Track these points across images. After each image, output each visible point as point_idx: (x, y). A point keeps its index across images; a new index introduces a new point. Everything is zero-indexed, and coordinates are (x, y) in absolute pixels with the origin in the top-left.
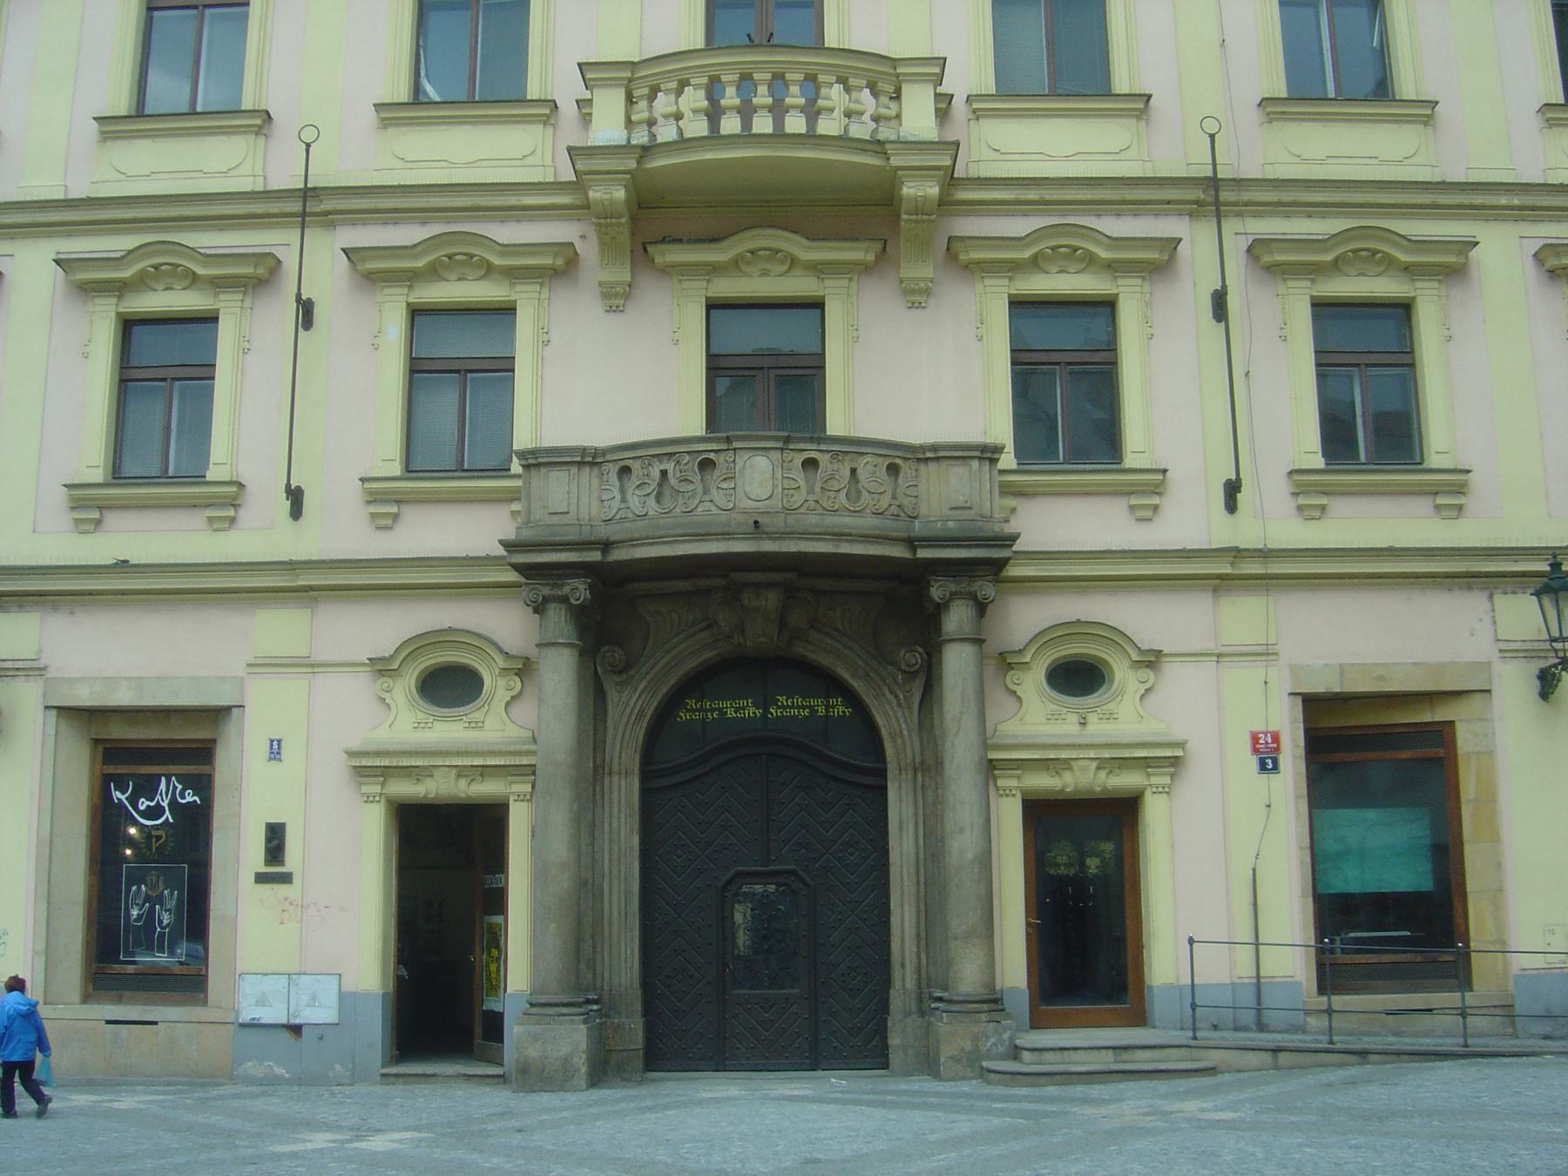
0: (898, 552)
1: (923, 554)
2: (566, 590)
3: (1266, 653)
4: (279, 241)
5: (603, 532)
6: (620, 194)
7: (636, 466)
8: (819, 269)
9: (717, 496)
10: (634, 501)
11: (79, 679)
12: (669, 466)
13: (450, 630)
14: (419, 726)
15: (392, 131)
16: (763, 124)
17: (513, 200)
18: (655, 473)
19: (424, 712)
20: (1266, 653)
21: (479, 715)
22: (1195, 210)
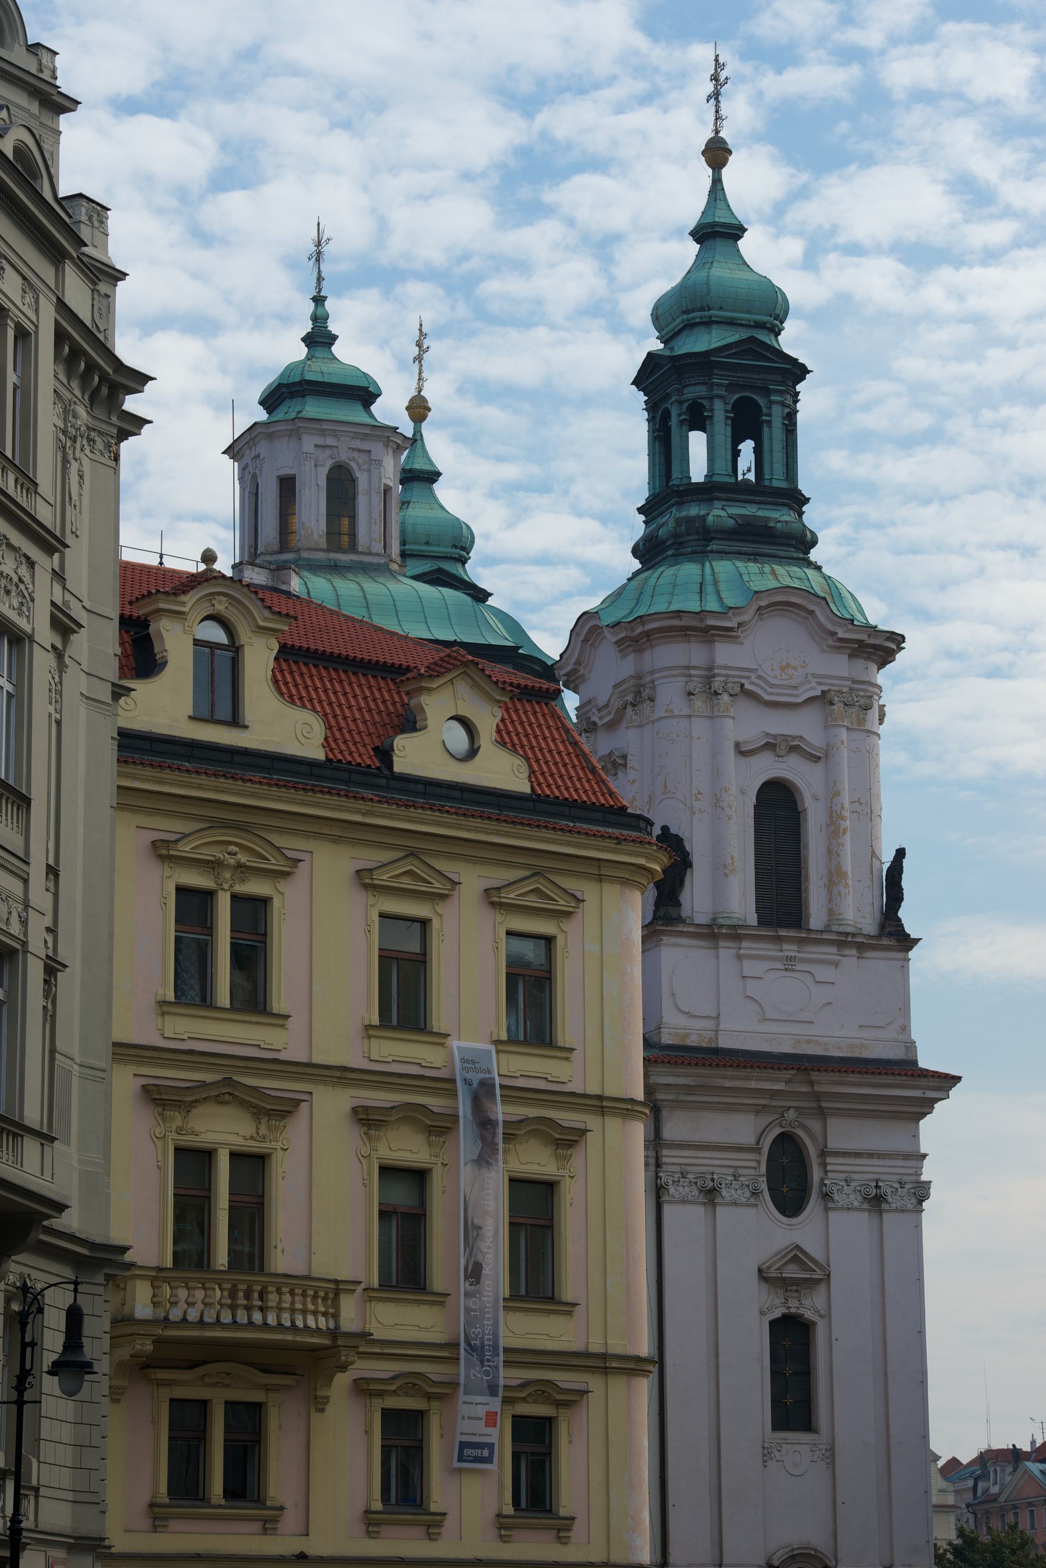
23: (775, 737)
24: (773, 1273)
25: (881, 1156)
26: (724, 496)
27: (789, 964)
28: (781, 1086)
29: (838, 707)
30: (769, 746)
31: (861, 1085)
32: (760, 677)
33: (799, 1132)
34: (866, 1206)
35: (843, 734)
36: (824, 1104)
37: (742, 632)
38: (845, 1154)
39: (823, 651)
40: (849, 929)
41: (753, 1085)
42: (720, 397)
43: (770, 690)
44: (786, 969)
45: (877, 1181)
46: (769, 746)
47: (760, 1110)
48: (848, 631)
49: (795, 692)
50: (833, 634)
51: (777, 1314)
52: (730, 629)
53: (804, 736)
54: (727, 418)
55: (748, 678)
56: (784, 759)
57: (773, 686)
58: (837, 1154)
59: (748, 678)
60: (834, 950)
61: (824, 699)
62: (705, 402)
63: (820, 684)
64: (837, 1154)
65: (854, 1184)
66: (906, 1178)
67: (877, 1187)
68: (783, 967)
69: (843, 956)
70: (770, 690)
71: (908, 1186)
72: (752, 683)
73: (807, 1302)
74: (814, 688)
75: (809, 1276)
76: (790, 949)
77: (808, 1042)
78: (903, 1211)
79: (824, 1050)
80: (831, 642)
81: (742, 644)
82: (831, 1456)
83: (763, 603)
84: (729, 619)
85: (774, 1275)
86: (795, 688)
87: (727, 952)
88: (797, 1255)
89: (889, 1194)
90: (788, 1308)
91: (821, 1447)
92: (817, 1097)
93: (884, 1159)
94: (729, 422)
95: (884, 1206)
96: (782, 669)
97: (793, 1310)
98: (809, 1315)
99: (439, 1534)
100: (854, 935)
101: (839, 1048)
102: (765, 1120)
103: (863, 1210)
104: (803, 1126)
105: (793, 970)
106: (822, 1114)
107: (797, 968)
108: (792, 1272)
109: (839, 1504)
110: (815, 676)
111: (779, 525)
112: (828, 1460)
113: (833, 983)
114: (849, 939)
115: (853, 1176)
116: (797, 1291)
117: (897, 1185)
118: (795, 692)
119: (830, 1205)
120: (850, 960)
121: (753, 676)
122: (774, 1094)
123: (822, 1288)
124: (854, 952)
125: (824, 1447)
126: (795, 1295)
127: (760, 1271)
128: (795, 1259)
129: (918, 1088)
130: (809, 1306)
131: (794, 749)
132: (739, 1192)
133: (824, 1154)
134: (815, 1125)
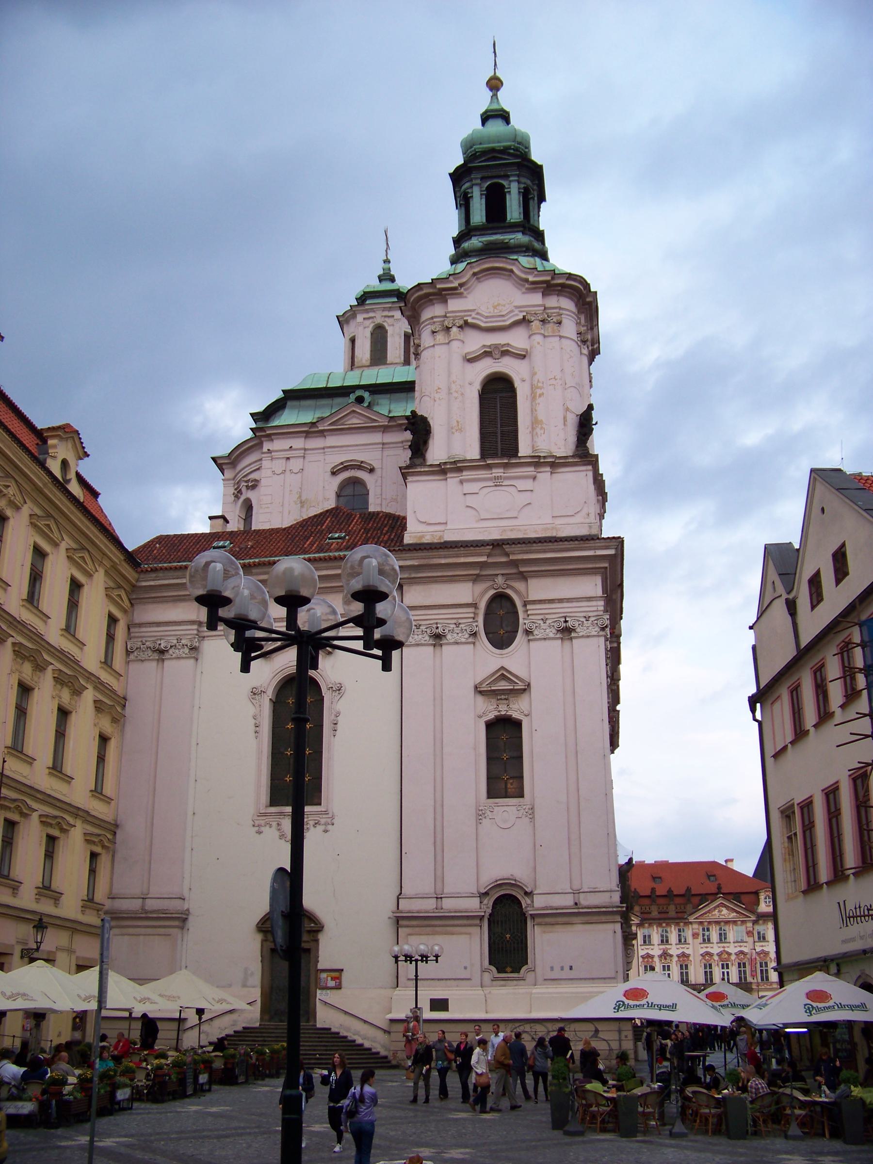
23: (490, 346)
24: (484, 687)
25: (569, 600)
26: (478, 233)
27: (497, 482)
28: (483, 559)
29: (536, 324)
30: (487, 354)
31: (545, 551)
32: (478, 314)
33: (509, 592)
34: (559, 635)
35: (538, 338)
36: (522, 569)
37: (465, 290)
38: (541, 602)
39: (524, 293)
40: (542, 455)
41: (462, 560)
42: (476, 184)
43: (485, 320)
44: (496, 486)
45: (565, 617)
46: (487, 354)
47: (476, 579)
48: (536, 276)
49: (503, 319)
50: (527, 280)
51: (491, 716)
52: (455, 289)
53: (510, 343)
54: (481, 195)
55: (470, 315)
56: (499, 360)
57: (487, 317)
58: (534, 602)
59: (470, 315)
60: (532, 469)
61: (524, 321)
62: (469, 191)
63: (521, 312)
64: (534, 602)
65: (548, 622)
66: (590, 614)
67: (566, 622)
68: (493, 484)
69: (540, 472)
70: (485, 320)
71: (592, 619)
72: (473, 318)
73: (514, 706)
74: (517, 315)
75: (512, 687)
76: (498, 472)
77: (512, 530)
78: (588, 637)
79: (524, 534)
80: (527, 286)
81: (466, 297)
82: (531, 812)
83: (476, 270)
84: (452, 282)
85: (486, 689)
86: (503, 316)
87: (453, 480)
88: (503, 674)
89: (577, 625)
90: (499, 711)
91: (524, 807)
92: (515, 563)
93: (572, 602)
94: (484, 197)
95: (573, 635)
96: (495, 307)
97: (503, 713)
98: (515, 715)
100: (545, 457)
101: (535, 531)
102: (480, 587)
103: (557, 639)
104: (509, 587)
105: (501, 486)
106: (523, 577)
107: (503, 484)
108: (503, 685)
109: (538, 846)
110: (516, 307)
111: (512, 241)
112: (531, 816)
113: (532, 491)
114: (542, 460)
115: (547, 616)
116: (506, 699)
117: (584, 620)
118: (503, 319)
119: (531, 637)
120: (544, 475)
121: (474, 315)
122: (482, 565)
123: (525, 696)
124: (548, 469)
125: (528, 807)
126: (505, 702)
127: (476, 687)
128: (503, 677)
129: (590, 549)
130: (516, 709)
131: (505, 353)
132: (460, 635)
133: (525, 604)
134: (519, 585)
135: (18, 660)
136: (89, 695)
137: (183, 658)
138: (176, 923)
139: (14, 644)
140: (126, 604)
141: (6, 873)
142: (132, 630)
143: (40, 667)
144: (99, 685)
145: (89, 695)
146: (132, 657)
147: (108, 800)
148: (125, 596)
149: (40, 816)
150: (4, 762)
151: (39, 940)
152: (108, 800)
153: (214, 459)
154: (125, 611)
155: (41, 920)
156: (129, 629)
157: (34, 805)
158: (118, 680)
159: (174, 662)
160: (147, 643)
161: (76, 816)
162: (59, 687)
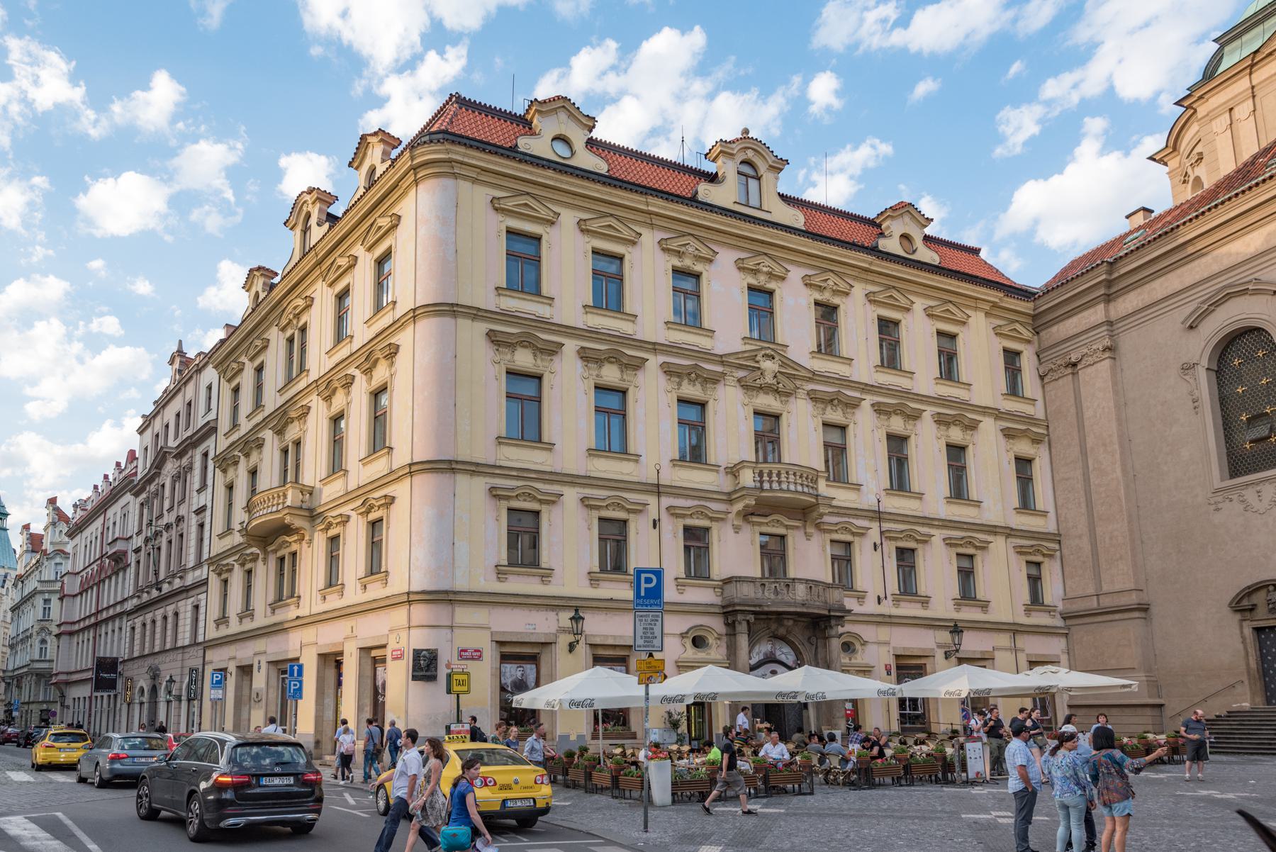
0: (826, 613)
1: (832, 614)
2: (748, 618)
3: (887, 643)
4: (652, 500)
5: (756, 602)
6: (754, 502)
7: (767, 584)
8: (787, 527)
9: (790, 594)
10: (766, 594)
11: (596, 635)
12: (778, 585)
13: (701, 626)
14: (694, 654)
15: (677, 468)
16: (784, 486)
17: (711, 496)
18: (773, 586)
19: (695, 650)
20: (887, 643)
21: (709, 651)
22: (871, 519)
99: (550, 581)
135: (882, 417)
136: (989, 427)
137: (1098, 362)
138: (1136, 614)
139: (873, 405)
140: (1026, 334)
141: (973, 596)
142: (1041, 356)
143: (915, 416)
144: (998, 414)
145: (989, 427)
146: (1046, 380)
147: (1044, 514)
148: (1021, 328)
149: (944, 540)
150: (879, 502)
151: (957, 642)
152: (1044, 514)
153: (1152, 158)
154: (1029, 342)
155: (956, 625)
156: (1038, 356)
157: (932, 531)
158: (1034, 405)
159: (1089, 370)
160: (1058, 362)
161: (995, 533)
162: (943, 428)
